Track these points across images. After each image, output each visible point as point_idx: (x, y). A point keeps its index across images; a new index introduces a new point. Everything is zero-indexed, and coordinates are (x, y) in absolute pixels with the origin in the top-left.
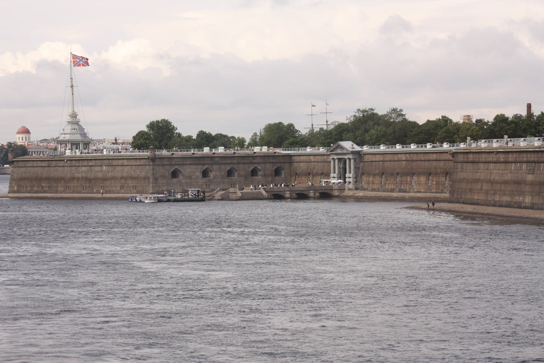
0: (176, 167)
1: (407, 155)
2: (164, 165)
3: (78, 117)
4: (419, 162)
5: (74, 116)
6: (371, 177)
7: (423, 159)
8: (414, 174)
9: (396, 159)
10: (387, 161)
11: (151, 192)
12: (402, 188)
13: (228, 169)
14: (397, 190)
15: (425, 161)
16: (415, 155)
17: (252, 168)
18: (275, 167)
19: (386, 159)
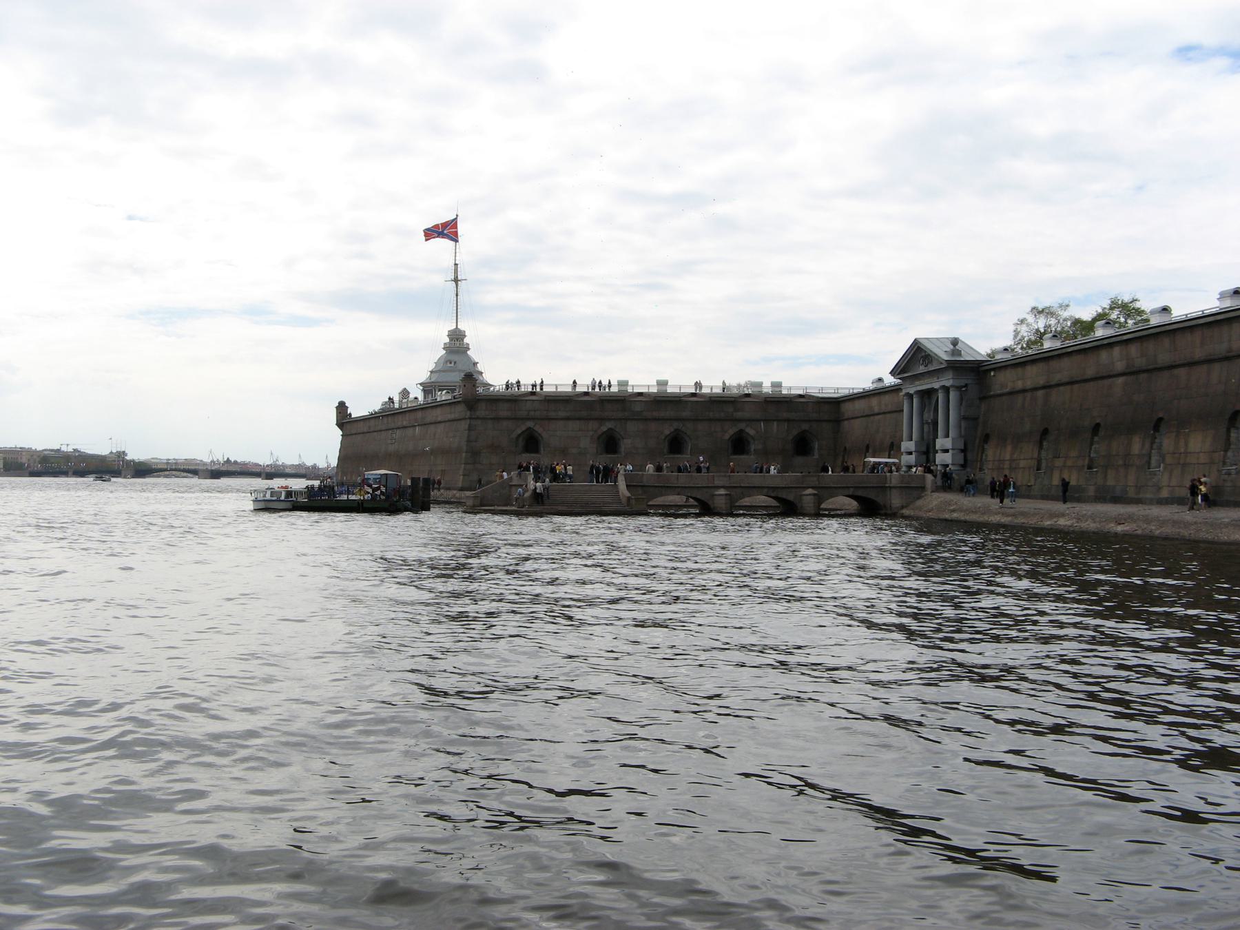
0: (530, 424)
1: (1134, 350)
2: (497, 419)
3: (466, 340)
4: (1182, 372)
5: (457, 337)
6: (1009, 448)
7: (1199, 354)
8: (1158, 425)
9: (1090, 372)
10: (1058, 385)
11: (460, 485)
12: (1111, 482)
13: (667, 432)
14: (1091, 491)
15: (1209, 361)
16: (1166, 341)
17: (731, 432)
18: (795, 432)
19: (1057, 378)
